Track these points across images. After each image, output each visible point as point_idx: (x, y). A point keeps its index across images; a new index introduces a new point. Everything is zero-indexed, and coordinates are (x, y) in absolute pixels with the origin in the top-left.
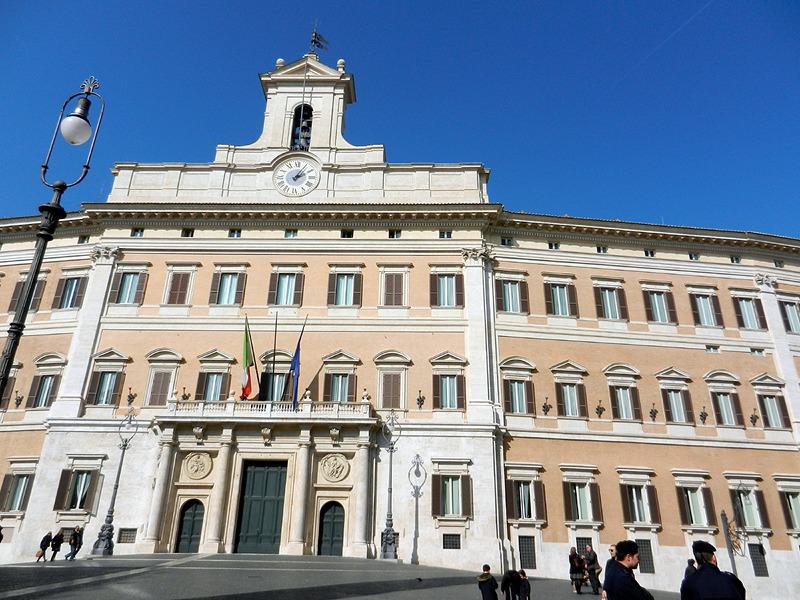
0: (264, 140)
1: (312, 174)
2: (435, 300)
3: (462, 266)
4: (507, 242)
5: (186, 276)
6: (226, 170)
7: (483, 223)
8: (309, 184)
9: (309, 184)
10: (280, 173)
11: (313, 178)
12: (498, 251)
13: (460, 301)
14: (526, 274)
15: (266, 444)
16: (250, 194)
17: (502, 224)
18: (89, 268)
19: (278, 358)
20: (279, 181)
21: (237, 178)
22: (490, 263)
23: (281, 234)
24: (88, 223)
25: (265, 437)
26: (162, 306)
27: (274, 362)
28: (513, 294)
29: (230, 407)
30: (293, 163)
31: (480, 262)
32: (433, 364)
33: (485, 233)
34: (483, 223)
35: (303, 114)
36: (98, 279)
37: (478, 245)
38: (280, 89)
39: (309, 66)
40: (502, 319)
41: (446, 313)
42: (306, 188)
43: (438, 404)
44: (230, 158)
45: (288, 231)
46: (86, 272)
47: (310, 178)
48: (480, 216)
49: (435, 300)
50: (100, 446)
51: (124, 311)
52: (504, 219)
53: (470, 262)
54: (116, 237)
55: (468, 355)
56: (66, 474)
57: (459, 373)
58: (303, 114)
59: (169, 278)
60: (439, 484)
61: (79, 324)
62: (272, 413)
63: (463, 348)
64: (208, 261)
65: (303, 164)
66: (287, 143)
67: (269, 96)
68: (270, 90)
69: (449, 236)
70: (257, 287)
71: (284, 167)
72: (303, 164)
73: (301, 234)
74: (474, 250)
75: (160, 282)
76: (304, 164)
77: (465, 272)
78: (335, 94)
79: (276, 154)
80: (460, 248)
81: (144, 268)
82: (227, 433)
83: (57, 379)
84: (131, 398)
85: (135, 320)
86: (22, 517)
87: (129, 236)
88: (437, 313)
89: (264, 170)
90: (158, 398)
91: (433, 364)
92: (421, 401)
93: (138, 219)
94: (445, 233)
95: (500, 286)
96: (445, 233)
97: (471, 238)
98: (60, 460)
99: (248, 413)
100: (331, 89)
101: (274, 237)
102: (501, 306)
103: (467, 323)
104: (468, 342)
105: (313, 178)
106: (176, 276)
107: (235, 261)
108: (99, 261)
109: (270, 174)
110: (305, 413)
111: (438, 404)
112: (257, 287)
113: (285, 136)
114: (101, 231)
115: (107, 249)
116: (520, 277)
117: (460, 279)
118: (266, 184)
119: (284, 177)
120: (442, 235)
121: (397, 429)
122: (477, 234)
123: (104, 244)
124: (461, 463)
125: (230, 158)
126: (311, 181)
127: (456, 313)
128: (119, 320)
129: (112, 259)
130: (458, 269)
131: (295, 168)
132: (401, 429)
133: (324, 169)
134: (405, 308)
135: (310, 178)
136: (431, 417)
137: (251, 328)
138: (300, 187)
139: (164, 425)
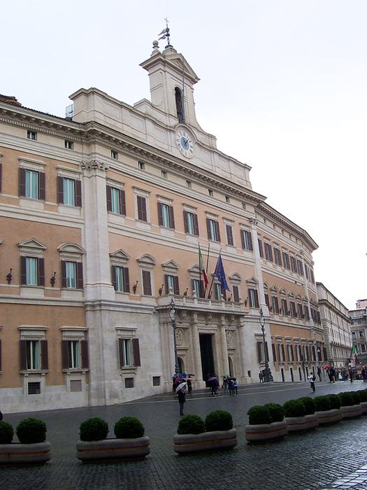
24: (81, 133)
29: (196, 301)
36: (95, 189)
38: (167, 69)
50: (131, 322)
56: (121, 341)
83: (79, 268)
84: (135, 288)
86: (88, 372)
89: (170, 130)
90: (148, 291)
91: (247, 282)
98: (112, 332)
107: (166, 196)
108: (98, 172)
110: (223, 307)
126: (192, 149)
138: (187, 152)
139: (161, 311)
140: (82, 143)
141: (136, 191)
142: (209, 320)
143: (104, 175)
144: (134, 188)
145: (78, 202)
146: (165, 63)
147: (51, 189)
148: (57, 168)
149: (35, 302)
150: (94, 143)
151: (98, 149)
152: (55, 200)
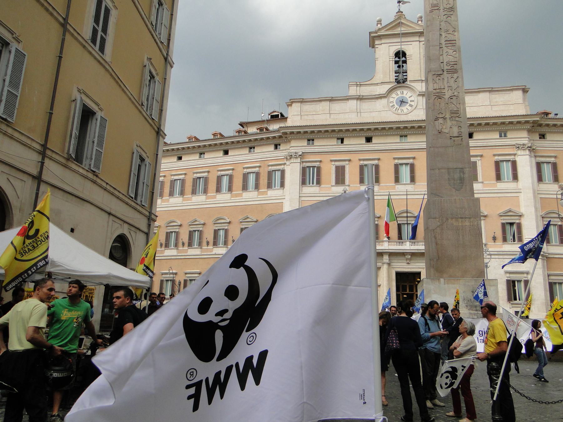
0: (379, 77)
1: (412, 99)
2: (498, 178)
3: (515, 155)
4: (542, 136)
5: (343, 167)
6: (357, 99)
7: (528, 126)
8: (411, 106)
9: (411, 106)
10: (391, 100)
11: (413, 101)
12: (540, 144)
13: (515, 177)
14: (555, 157)
15: (408, 263)
16: (374, 114)
17: (540, 125)
18: (285, 164)
19: (409, 215)
20: (391, 104)
21: (366, 105)
22: (531, 149)
23: (397, 139)
24: (280, 137)
25: (407, 259)
26: (332, 186)
27: (407, 217)
28: (547, 171)
30: (399, 92)
31: (527, 152)
32: (501, 216)
33: (529, 131)
34: (528, 126)
35: (400, 56)
36: (293, 172)
37: (525, 141)
38: (383, 41)
39: (402, 23)
40: (543, 186)
41: (506, 185)
42: (409, 108)
43: (505, 240)
44: (358, 91)
45: (401, 136)
46: (282, 166)
47: (411, 101)
48: (527, 122)
49: (498, 178)
51: (311, 189)
52: (542, 122)
53: (519, 152)
54: (298, 146)
55: (523, 210)
57: (518, 221)
58: (400, 56)
59: (334, 168)
60: (511, 285)
61: (287, 198)
62: (407, 246)
63: (519, 206)
64: (355, 158)
65: (405, 92)
66: (393, 79)
67: (376, 46)
68: (377, 42)
69: (505, 136)
70: (387, 173)
71: (394, 95)
72: (405, 92)
73: (410, 139)
74: (524, 145)
75: (329, 172)
76: (406, 94)
77: (518, 159)
78: (420, 41)
79: (387, 87)
80: (514, 143)
81: (318, 163)
82: (386, 258)
85: (319, 195)
87: (306, 144)
88: (500, 186)
89: (381, 98)
91: (501, 216)
92: (494, 239)
93: (310, 134)
94: (503, 134)
95: (539, 166)
96: (503, 134)
97: (521, 137)
99: (395, 247)
100: (417, 39)
101: (393, 142)
102: (540, 179)
103: (520, 191)
104: (523, 203)
105: (413, 101)
106: (337, 168)
108: (292, 161)
109: (384, 101)
111: (505, 240)
112: (387, 173)
113: (391, 73)
114: (289, 141)
115: (296, 153)
116: (552, 160)
117: (514, 164)
118: (383, 107)
119: (395, 102)
120: (501, 136)
121: (488, 255)
122: (525, 134)
123: (293, 150)
124: (523, 273)
125: (358, 91)
126: (412, 103)
127: (512, 185)
128: (310, 195)
129: (299, 159)
130: (513, 157)
131: (400, 95)
132: (491, 255)
133: (419, 95)
134: (480, 183)
135: (411, 101)
136: (502, 247)
137: (392, 197)
140: (286, 142)
141: (333, 163)
142: (410, 259)
143: (299, 160)
144: (331, 161)
145: (282, 185)
146: (380, 37)
147: (264, 181)
148: (269, 166)
149: (193, 257)
150: (291, 139)
151: (293, 143)
152: (266, 187)
